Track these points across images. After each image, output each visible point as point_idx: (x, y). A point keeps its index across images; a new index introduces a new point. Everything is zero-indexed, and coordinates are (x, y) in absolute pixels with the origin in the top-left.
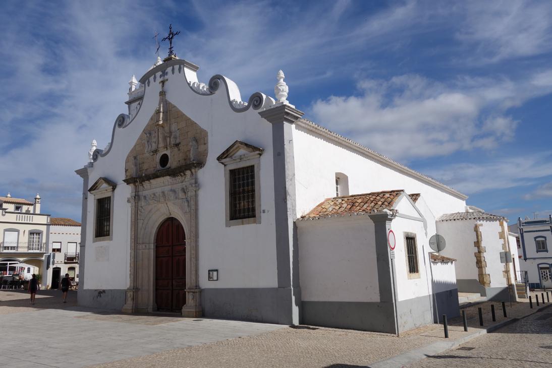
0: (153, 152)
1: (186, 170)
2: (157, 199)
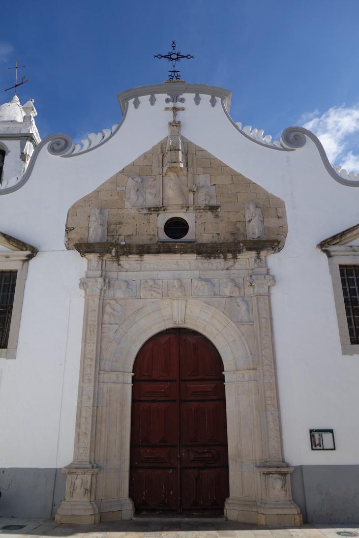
0: (150, 209)
1: (229, 252)
2: (160, 291)
